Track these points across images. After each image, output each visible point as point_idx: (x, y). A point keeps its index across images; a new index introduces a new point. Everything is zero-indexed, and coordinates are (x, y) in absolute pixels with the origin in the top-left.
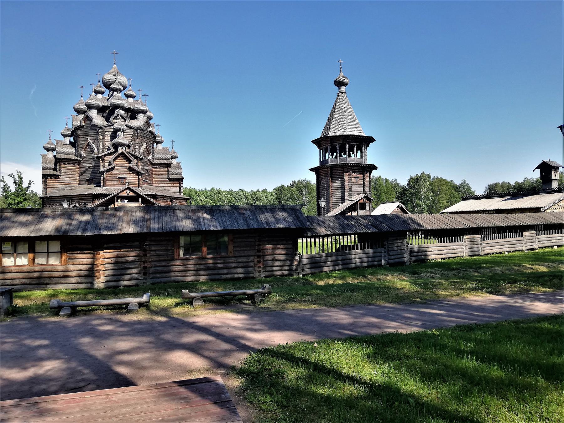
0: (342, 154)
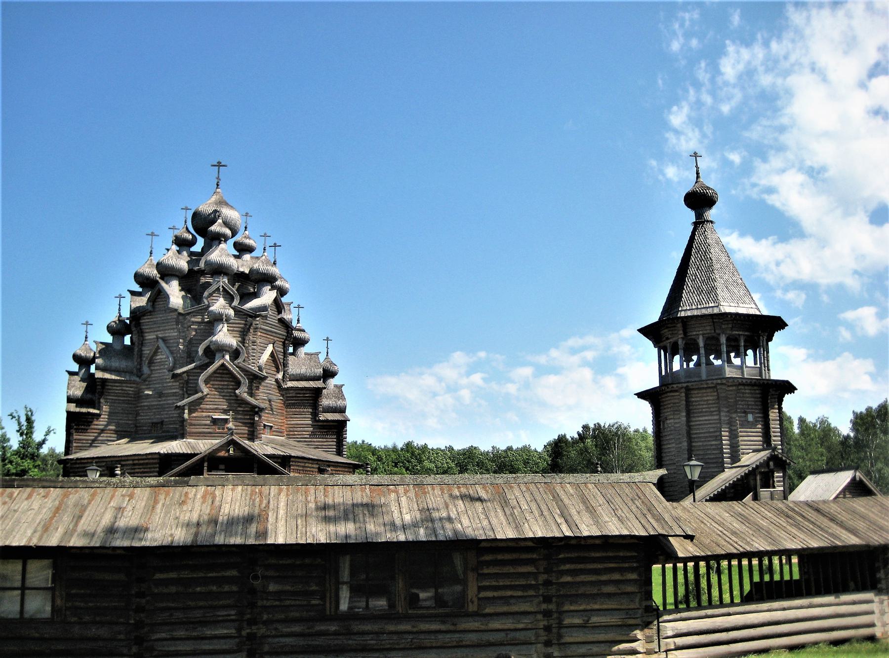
0: (712, 357)
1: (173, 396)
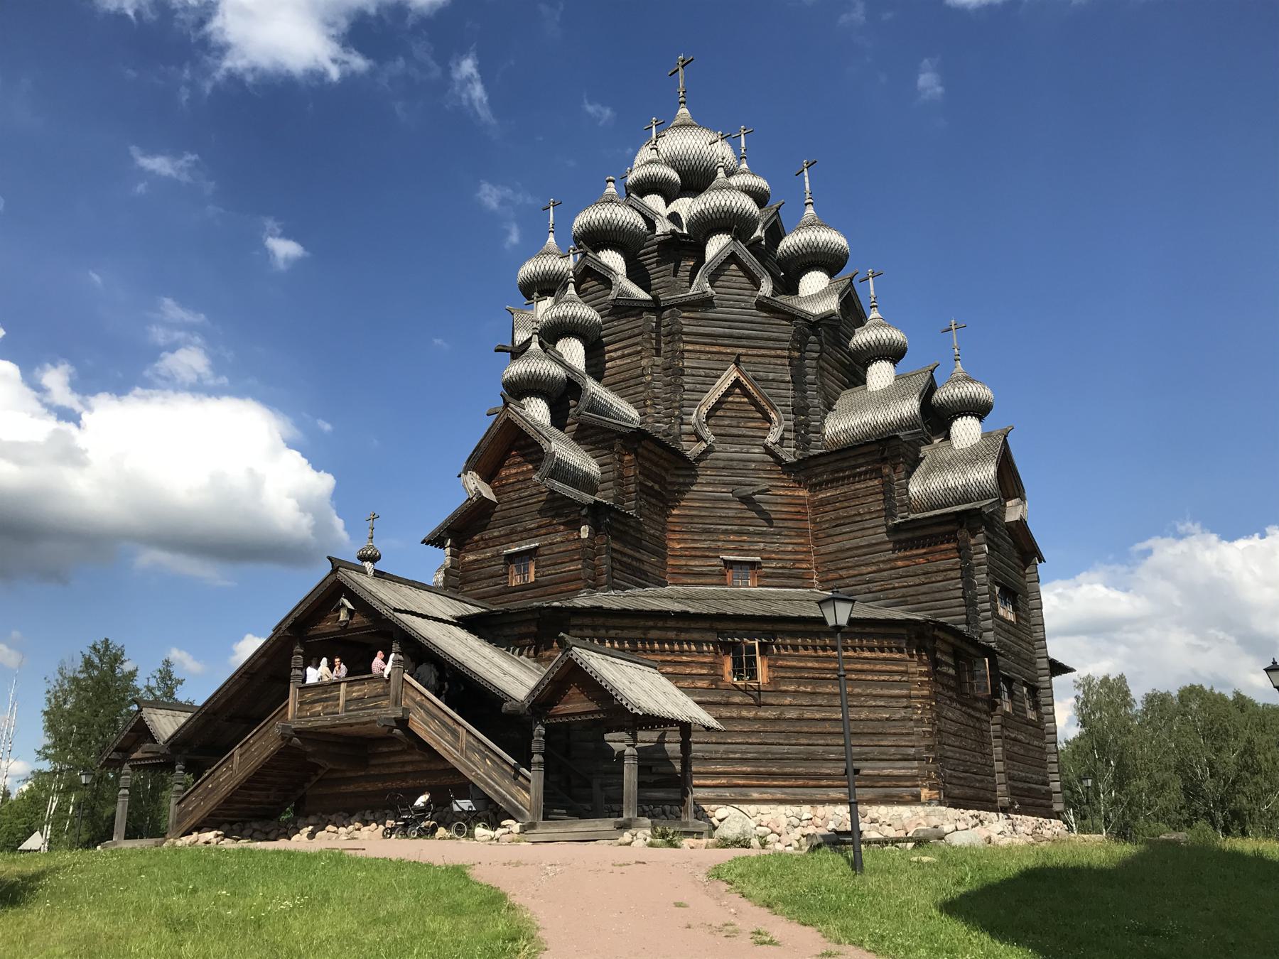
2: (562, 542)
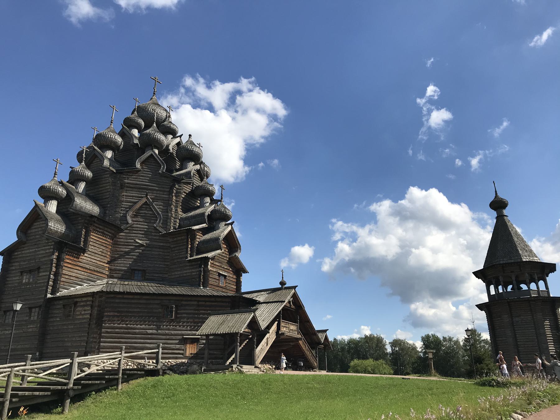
1: (159, 248)
2: (231, 277)
